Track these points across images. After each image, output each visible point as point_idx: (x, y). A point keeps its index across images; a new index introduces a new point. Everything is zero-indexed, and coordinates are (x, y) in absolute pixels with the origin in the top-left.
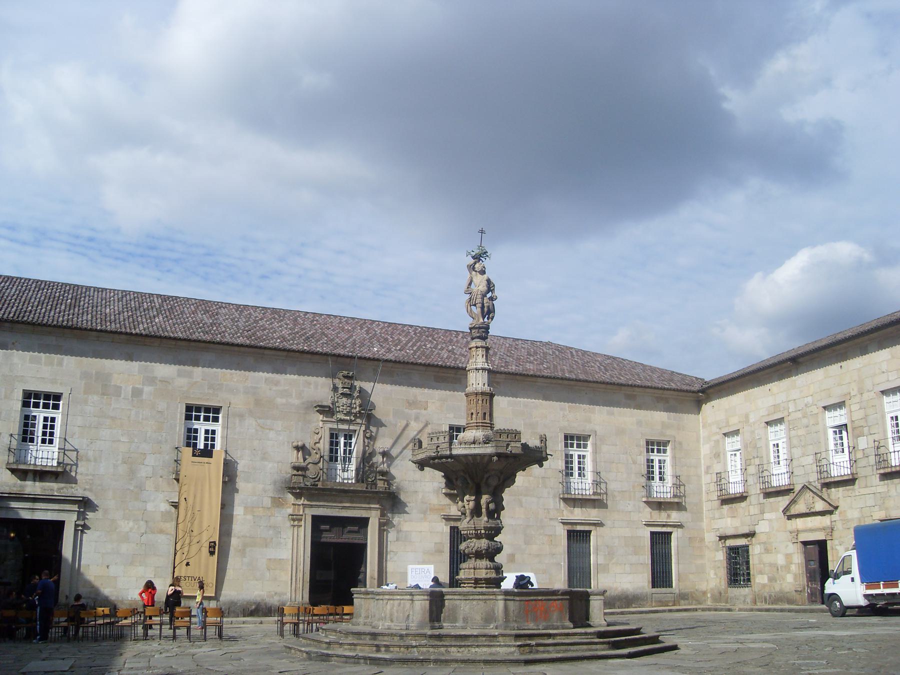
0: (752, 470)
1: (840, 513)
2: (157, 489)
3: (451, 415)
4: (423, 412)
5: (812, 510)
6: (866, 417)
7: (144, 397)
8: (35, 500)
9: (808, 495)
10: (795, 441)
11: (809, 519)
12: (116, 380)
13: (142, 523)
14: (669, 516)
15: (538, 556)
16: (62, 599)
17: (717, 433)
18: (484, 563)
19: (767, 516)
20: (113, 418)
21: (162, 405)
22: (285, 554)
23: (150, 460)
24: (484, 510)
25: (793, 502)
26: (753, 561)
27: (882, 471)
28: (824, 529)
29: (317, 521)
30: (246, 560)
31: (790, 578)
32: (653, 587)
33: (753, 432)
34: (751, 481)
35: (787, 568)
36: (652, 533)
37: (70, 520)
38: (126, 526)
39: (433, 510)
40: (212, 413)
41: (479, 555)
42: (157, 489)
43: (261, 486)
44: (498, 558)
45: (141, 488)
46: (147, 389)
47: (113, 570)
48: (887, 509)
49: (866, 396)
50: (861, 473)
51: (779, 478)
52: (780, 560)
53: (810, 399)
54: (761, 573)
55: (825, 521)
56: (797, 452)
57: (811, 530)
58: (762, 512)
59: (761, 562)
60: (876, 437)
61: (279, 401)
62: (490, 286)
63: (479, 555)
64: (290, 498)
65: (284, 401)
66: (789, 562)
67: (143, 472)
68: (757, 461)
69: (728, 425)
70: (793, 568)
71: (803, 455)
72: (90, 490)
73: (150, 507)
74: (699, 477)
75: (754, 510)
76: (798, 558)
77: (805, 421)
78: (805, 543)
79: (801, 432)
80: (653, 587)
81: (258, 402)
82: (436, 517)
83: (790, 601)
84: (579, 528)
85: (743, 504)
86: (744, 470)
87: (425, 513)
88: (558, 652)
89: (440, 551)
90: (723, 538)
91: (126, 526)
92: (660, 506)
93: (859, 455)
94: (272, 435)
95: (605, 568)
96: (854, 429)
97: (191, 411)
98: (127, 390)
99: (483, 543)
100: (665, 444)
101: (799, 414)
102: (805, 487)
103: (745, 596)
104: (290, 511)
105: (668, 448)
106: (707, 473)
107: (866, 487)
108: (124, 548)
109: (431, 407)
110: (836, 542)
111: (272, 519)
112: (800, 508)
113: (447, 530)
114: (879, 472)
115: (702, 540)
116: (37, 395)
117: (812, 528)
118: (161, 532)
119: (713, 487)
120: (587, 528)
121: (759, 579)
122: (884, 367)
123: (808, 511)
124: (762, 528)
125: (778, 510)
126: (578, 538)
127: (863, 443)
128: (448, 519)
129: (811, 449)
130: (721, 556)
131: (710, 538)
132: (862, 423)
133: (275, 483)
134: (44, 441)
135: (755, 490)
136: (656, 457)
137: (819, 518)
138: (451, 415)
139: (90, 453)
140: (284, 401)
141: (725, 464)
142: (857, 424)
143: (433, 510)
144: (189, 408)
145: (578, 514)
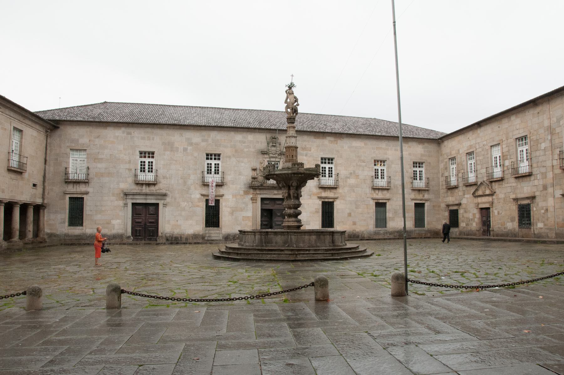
0: (460, 175)
2: (196, 189)
3: (322, 153)
4: (309, 152)
6: (509, 151)
7: (188, 151)
8: (146, 195)
9: (483, 187)
10: (478, 162)
12: (176, 145)
13: (190, 203)
14: (424, 196)
15: (361, 213)
16: (160, 234)
17: (446, 158)
18: (293, 219)
19: (466, 196)
20: (176, 161)
21: (196, 154)
22: (250, 214)
23: (192, 177)
24: (292, 197)
25: (477, 190)
26: (460, 216)
28: (489, 202)
29: (263, 200)
30: (234, 217)
31: (474, 224)
32: (415, 227)
33: (461, 158)
36: (415, 203)
37: (161, 203)
38: (183, 204)
40: (217, 156)
41: (290, 216)
42: (196, 189)
43: (239, 186)
44: (299, 217)
45: (189, 189)
46: (189, 148)
47: (179, 223)
49: (509, 141)
50: (506, 177)
51: (472, 178)
52: (471, 216)
53: (485, 143)
54: (463, 222)
55: (490, 199)
56: (479, 167)
57: (484, 203)
58: (464, 195)
59: (463, 216)
60: (513, 160)
61: (246, 150)
62: (296, 100)
63: (290, 216)
64: (252, 191)
65: (247, 150)
66: (474, 217)
67: (190, 182)
68: (462, 171)
69: (451, 155)
70: (476, 220)
71: (482, 168)
72: (168, 190)
73: (193, 196)
74: (439, 178)
75: (461, 193)
76: (478, 216)
77: (483, 153)
78: (482, 209)
79: (481, 158)
80: (415, 227)
81: (236, 151)
82: (316, 197)
83: (475, 235)
84: (381, 201)
85: (456, 190)
86: (457, 175)
87: (310, 196)
88: (308, 257)
89: (317, 212)
90: (448, 206)
91: (183, 204)
92: (419, 190)
93: (505, 168)
94: (243, 164)
95: (393, 219)
96: (503, 156)
97: (209, 156)
98: (181, 149)
99: (291, 211)
100: (422, 163)
101: (480, 150)
103: (456, 232)
104: (251, 196)
105: (424, 165)
106: (442, 176)
108: (183, 213)
109: (313, 150)
110: (494, 208)
111: (244, 200)
112: (480, 192)
113: (321, 203)
115: (439, 206)
116: (145, 153)
117: (484, 202)
118: (198, 206)
119: (444, 183)
120: (384, 201)
121: (462, 225)
122: (518, 127)
124: (464, 201)
126: (381, 205)
127: (507, 163)
128: (320, 198)
129: (485, 166)
130: (447, 214)
131: (443, 205)
132: (507, 153)
133: (245, 184)
134: (149, 171)
135: (461, 185)
136: (418, 169)
137: (487, 197)
138: (322, 153)
139: (168, 175)
140: (247, 150)
141: (449, 172)
142: (504, 154)
143: (314, 194)
144: (207, 155)
145: (380, 195)
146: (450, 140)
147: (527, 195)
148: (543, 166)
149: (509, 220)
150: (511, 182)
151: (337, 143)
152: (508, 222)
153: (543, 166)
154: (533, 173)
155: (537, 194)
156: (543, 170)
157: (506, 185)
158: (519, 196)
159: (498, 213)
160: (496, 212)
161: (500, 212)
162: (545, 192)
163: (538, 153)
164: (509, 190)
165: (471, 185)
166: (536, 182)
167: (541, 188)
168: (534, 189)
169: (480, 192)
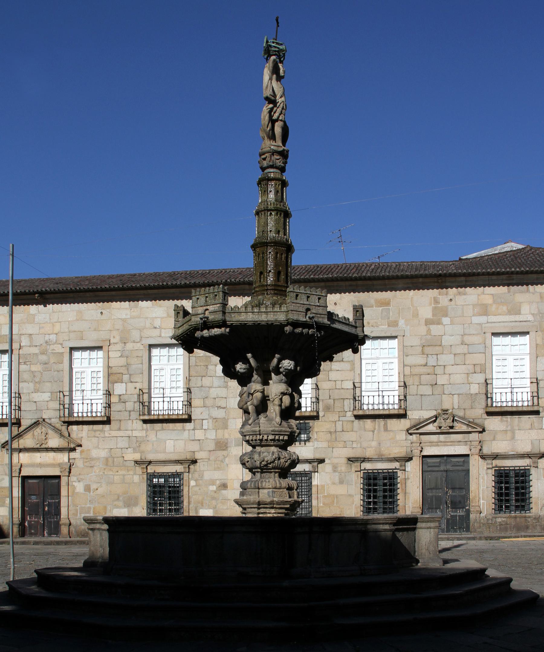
1: (82, 452)
5: (44, 446)
11: (38, 455)
27: (146, 417)
28: (60, 465)
48: (142, 452)
55: (63, 457)
57: (40, 465)
60: (139, 386)
107: (119, 429)
110: (73, 478)
114: (142, 418)
123: (38, 446)
127: (119, 389)
147: (177, 458)
148: (219, 407)
149: (121, 504)
150: (137, 429)
152: (117, 507)
153: (219, 407)
154: (193, 418)
155: (198, 456)
156: (220, 414)
157: (114, 433)
158: (150, 457)
159: (87, 488)
160: (79, 487)
161: (93, 486)
162: (220, 453)
163: (206, 381)
164: (122, 443)
166: (199, 435)
167: (212, 446)
168: (194, 447)
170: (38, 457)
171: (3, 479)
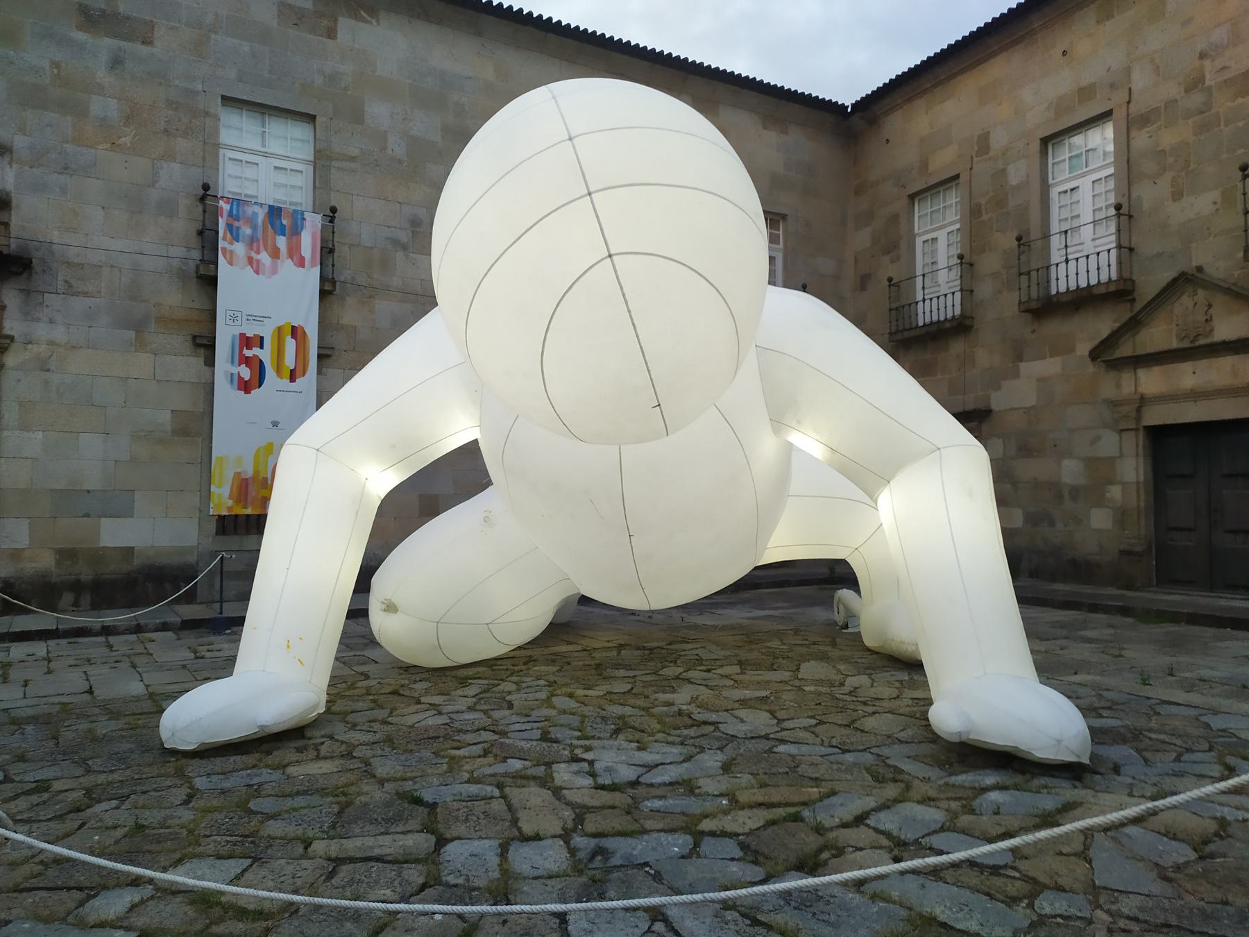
5: (1202, 341)
9: (1186, 304)
11: (1186, 367)
25: (1134, 324)
31: (1100, 519)
34: (985, 290)
35: (1092, 492)
39: (167, 322)
52: (1070, 471)
57: (1195, 395)
70: (1115, 492)
76: (1133, 469)
87: (139, 326)
102: (1185, 281)
123: (1186, 344)
125: (1072, 350)
135: (1000, 307)
146: (920, 103)
151: (331, 33)
165: (1084, 300)
169: (1158, 335)
170: (1189, 376)
171: (1098, 438)
